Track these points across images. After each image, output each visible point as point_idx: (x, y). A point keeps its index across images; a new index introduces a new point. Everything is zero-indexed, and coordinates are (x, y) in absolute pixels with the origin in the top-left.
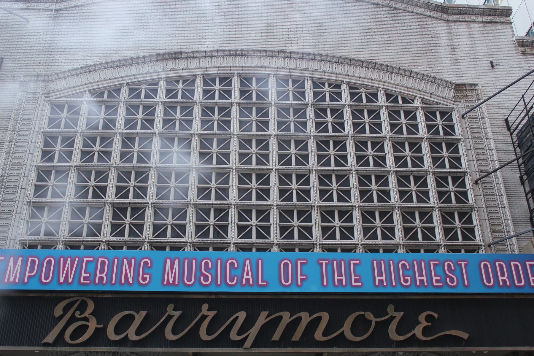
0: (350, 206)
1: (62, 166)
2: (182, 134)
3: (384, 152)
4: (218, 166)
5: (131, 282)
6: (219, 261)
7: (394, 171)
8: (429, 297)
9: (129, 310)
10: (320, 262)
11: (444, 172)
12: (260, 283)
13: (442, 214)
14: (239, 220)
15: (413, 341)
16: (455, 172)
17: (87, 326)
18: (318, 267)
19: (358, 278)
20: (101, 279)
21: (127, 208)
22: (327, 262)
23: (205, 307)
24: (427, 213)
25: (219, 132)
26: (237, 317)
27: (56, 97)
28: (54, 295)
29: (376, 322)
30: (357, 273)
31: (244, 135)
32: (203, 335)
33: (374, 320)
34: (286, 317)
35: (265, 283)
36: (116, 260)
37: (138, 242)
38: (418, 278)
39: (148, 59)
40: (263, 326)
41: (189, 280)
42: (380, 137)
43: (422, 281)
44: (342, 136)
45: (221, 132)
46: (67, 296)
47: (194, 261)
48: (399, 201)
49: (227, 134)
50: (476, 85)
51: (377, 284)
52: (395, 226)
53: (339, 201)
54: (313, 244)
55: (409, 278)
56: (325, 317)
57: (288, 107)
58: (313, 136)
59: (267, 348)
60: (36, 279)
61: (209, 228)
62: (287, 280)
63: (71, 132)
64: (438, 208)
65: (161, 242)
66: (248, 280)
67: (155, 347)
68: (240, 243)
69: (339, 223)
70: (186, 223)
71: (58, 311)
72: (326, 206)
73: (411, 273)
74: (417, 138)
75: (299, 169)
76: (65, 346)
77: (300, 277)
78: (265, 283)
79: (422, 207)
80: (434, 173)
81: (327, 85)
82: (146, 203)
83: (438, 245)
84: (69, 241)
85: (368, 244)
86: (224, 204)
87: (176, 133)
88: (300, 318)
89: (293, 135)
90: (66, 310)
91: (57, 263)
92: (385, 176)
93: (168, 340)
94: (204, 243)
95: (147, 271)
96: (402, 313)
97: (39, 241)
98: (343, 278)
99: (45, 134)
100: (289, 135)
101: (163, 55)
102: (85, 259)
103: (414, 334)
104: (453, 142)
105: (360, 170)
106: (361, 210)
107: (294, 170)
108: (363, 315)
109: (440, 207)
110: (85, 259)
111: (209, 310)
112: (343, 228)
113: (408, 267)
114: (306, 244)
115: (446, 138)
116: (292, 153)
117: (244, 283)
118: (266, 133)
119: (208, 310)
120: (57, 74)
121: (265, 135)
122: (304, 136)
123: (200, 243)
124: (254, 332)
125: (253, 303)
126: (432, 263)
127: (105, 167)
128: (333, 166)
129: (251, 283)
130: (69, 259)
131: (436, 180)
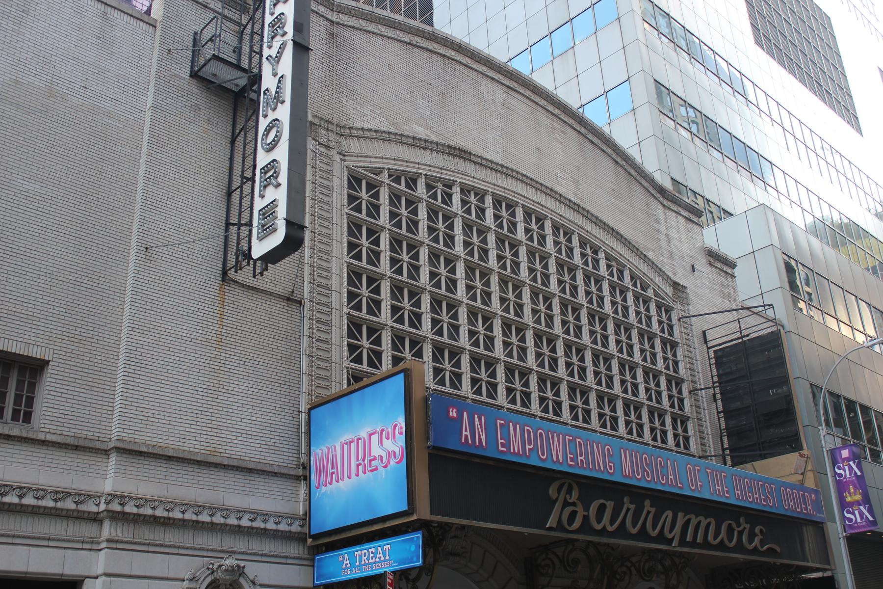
50: (686, 288)
60: (534, 454)
71: (552, 492)
81: (588, 246)
90: (559, 490)
101: (454, 148)
120: (350, 128)
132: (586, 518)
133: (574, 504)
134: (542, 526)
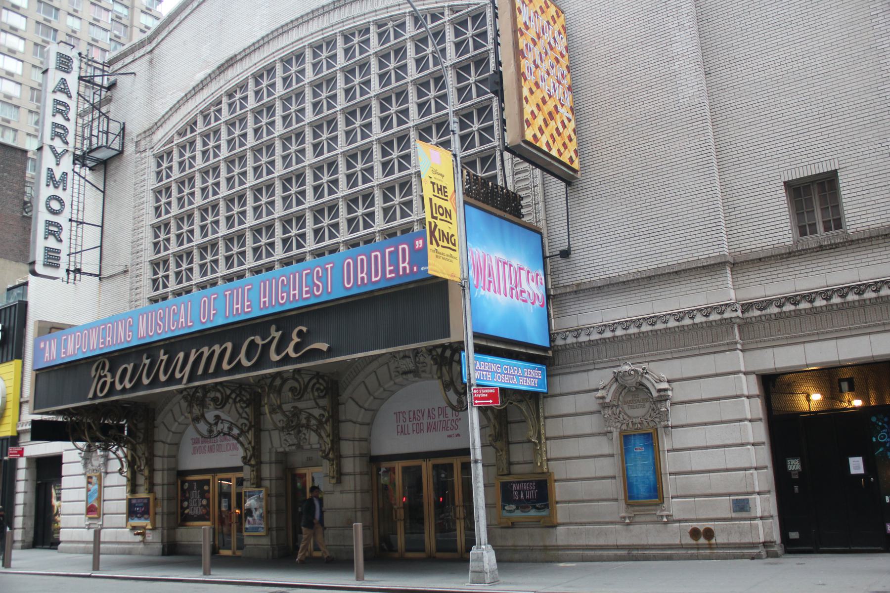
15: (287, 360)
39: (213, 76)
56: (229, 345)
90: (97, 370)
103: (287, 353)
132: (113, 384)
134: (85, 399)
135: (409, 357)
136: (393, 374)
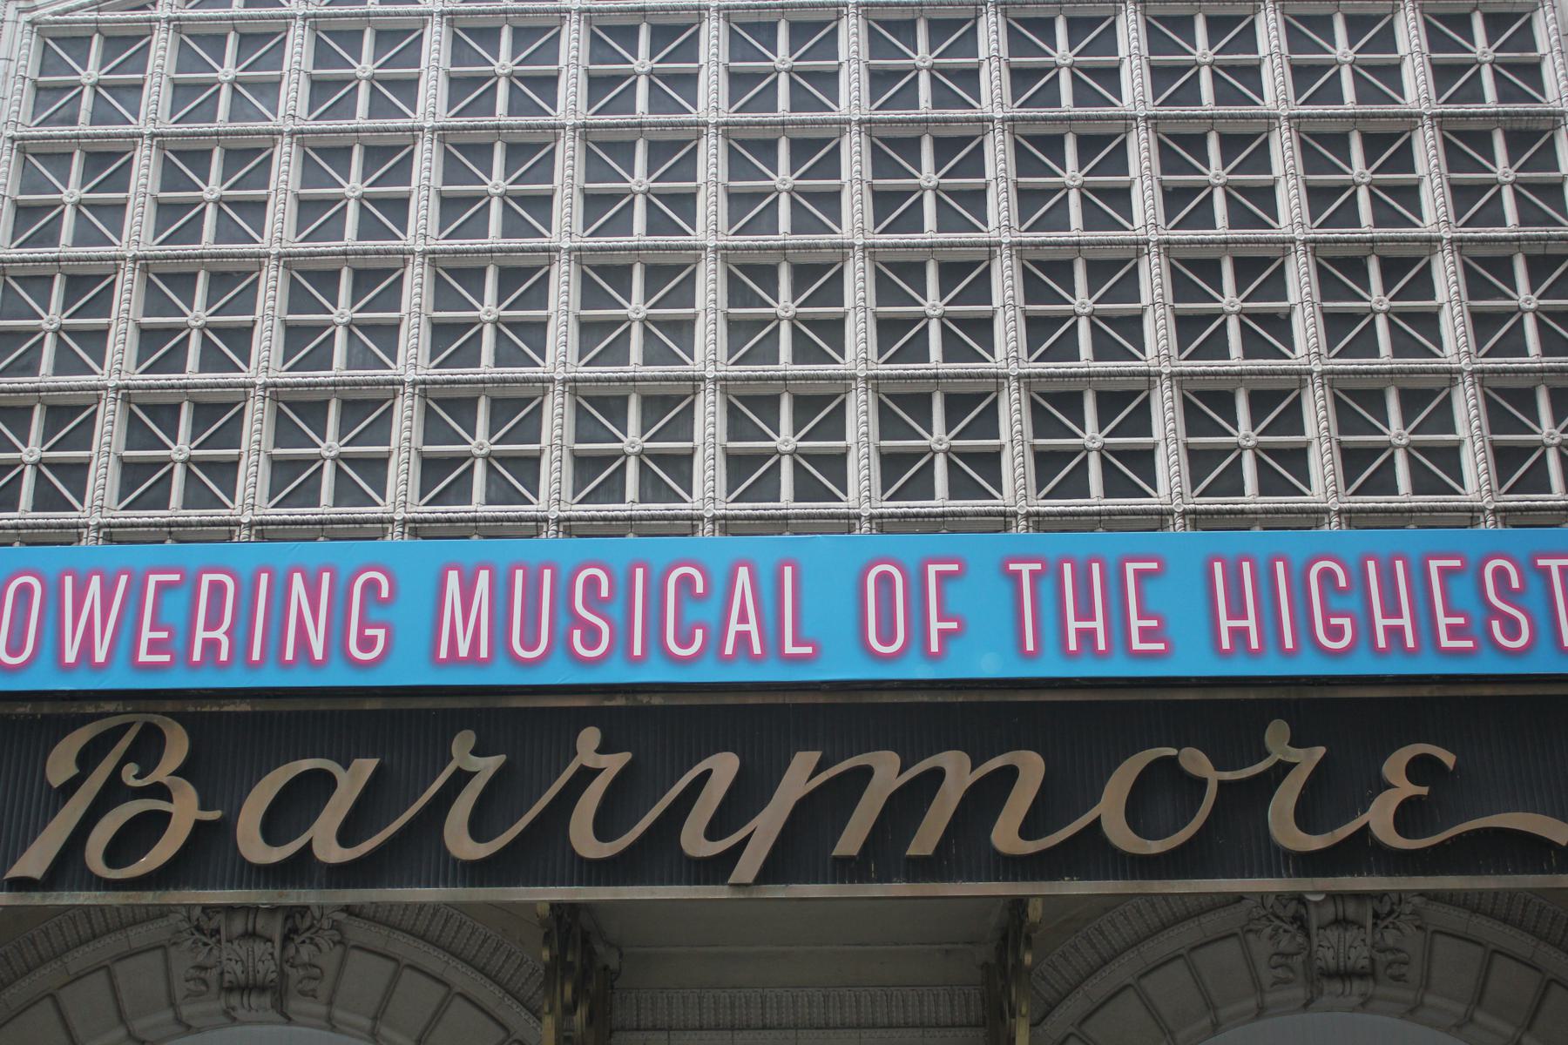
0: (1141, 374)
1: (89, 259)
2: (519, 127)
3: (1269, 172)
4: (651, 240)
5: (318, 655)
6: (639, 572)
7: (1305, 242)
8: (1424, 692)
9: (313, 756)
10: (1013, 567)
11: (1495, 240)
12: (789, 649)
13: (1486, 397)
14: (733, 435)
16: (1539, 238)
17: (165, 817)
18: (1005, 589)
19: (1154, 623)
20: (211, 646)
21: (326, 403)
22: (1038, 566)
23: (589, 738)
24: (1430, 394)
25: (653, 118)
26: (707, 774)
27: (56, 8)
28: (46, 708)
29: (1221, 784)
30: (1152, 606)
31: (749, 124)
32: (585, 842)
33: (1213, 777)
34: (888, 771)
35: (809, 650)
36: (264, 577)
37: (366, 521)
38: (1380, 623)
40: (802, 806)
41: (530, 643)
42: (1254, 117)
43: (1395, 633)
44: (1110, 118)
45: (663, 118)
46: (90, 709)
47: (547, 573)
48: (1323, 350)
49: (683, 124)
51: (1226, 645)
52: (1309, 443)
53: (1098, 357)
54: (1003, 514)
55: (1346, 622)
56: (1031, 767)
57: (910, 17)
58: (1003, 120)
59: (816, 882)
61: (623, 466)
62: (887, 637)
63: (119, 136)
64: (1472, 373)
65: (449, 520)
66: (743, 637)
67: (410, 885)
68: (736, 518)
69: (1100, 437)
70: (541, 451)
71: (60, 765)
72: (1051, 376)
73: (1354, 603)
74: (1396, 115)
75: (951, 245)
76: (89, 889)
77: (935, 626)
78: (809, 650)
79: (1412, 371)
80: (1459, 244)
82: (392, 383)
83: (1471, 510)
84: (121, 526)
85: (1207, 512)
86: (678, 379)
87: (498, 127)
88: (937, 775)
89: (926, 120)
90: (88, 759)
91: (54, 594)
92: (1271, 261)
93: (455, 860)
94: (604, 519)
95: (375, 614)
96: (1320, 751)
97: (16, 527)
98: (1098, 624)
99: (22, 147)
100: (912, 121)
102: (153, 579)
103: (1366, 827)
104: (1534, 126)
105: (1179, 242)
106: (1181, 388)
107: (931, 246)
108: (1174, 759)
109: (1482, 371)
110: (153, 579)
111: (603, 749)
112: (1115, 454)
113: (1342, 583)
114: (977, 514)
115: (1506, 114)
116: (924, 184)
117: (729, 650)
118: (826, 115)
119: (603, 749)
121: (825, 122)
122: (968, 120)
123: (593, 519)
124: (767, 825)
125: (765, 720)
126: (1434, 565)
127: (244, 256)
128: (1076, 229)
129: (757, 650)
130: (96, 580)
131: (1467, 269)
133: (161, 791)
135: (1361, 926)
136: (1267, 976)
